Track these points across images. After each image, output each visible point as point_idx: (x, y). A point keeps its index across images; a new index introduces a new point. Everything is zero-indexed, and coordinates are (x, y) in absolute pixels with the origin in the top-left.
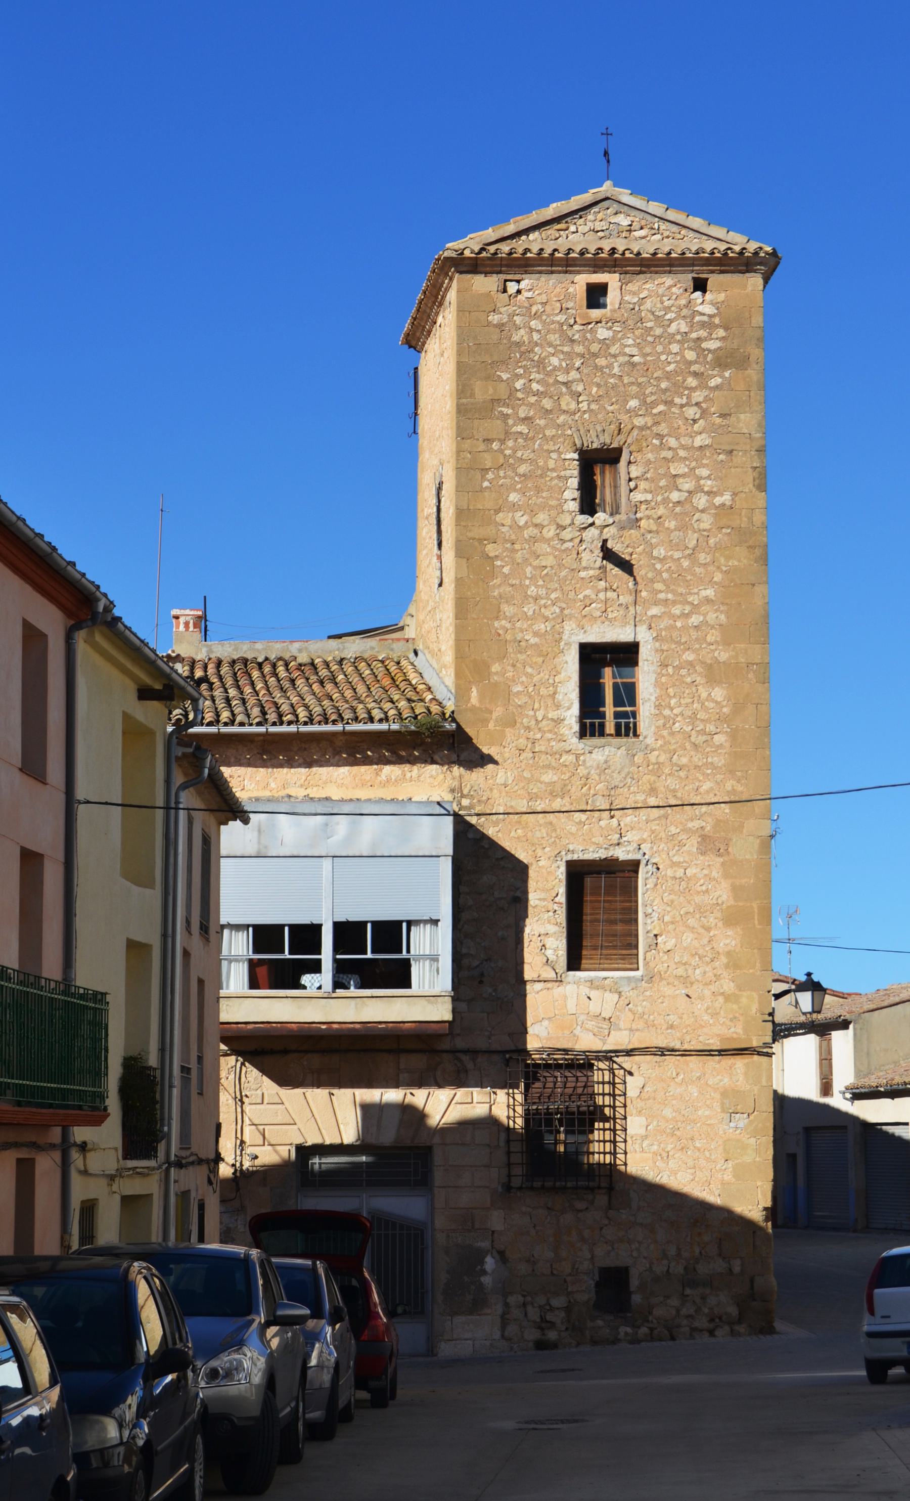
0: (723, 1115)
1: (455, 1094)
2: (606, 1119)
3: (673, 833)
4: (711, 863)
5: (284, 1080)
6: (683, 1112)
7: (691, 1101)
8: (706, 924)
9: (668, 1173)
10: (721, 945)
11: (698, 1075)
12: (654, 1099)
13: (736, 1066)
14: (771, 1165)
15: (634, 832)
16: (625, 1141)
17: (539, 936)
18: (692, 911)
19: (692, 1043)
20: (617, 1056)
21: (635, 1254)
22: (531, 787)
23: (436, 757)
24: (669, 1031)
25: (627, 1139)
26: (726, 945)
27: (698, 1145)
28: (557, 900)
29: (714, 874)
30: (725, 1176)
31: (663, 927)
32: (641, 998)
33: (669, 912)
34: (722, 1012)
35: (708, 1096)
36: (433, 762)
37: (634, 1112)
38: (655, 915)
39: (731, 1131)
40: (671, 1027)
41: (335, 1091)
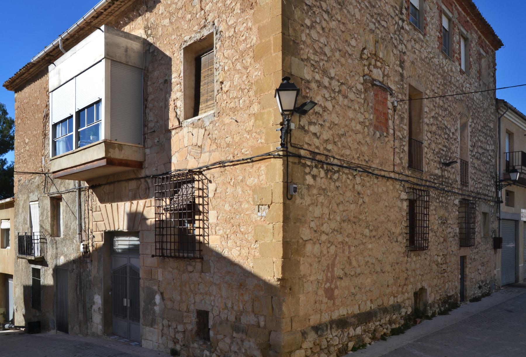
0: (254, 207)
1: (146, 202)
2: (199, 213)
3: (228, 4)
4: (247, 17)
5: (102, 201)
6: (234, 206)
7: (238, 198)
8: (246, 64)
9: (227, 249)
10: (253, 77)
11: (241, 178)
12: (221, 198)
13: (262, 168)
14: (282, 245)
15: (210, 14)
16: (208, 228)
17: (174, 101)
18: (238, 57)
19: (238, 155)
20: (204, 170)
21: (213, 304)
22: (171, 9)
23: (140, 12)
24: (227, 149)
25: (210, 226)
26: (256, 76)
27: (242, 230)
28: (181, 76)
29: (250, 24)
30: (256, 253)
31: (224, 75)
32: (214, 128)
33: (227, 63)
34: (254, 129)
35: (247, 194)
36: (140, 15)
37: (212, 207)
38: (221, 68)
39: (259, 219)
40: (228, 145)
41: (113, 204)
